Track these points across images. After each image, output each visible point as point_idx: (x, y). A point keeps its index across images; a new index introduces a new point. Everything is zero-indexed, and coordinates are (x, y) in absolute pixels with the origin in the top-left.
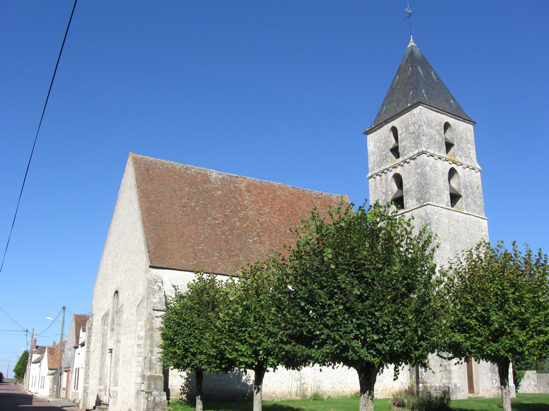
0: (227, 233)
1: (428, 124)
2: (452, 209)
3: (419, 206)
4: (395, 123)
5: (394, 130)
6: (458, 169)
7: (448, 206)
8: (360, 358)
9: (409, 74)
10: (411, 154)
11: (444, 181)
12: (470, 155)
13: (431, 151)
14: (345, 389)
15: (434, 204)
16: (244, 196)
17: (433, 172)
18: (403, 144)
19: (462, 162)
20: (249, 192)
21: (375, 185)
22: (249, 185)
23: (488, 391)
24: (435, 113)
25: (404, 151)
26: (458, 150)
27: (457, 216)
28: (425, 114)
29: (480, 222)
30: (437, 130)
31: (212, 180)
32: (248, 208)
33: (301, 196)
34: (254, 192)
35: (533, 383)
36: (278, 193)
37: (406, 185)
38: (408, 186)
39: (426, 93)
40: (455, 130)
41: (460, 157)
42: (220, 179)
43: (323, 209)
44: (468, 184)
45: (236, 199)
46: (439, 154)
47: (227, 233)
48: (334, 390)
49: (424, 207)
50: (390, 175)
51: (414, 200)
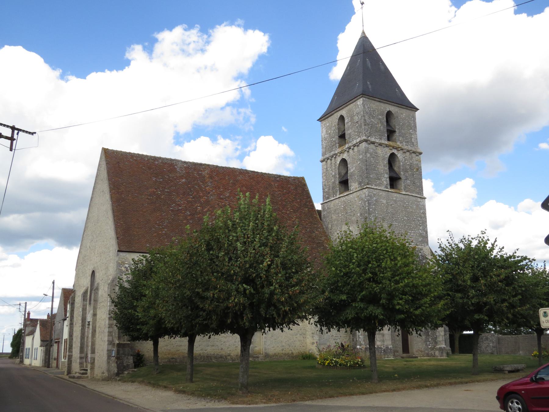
0: (189, 218)
1: (370, 114)
2: (393, 190)
3: (360, 188)
4: (343, 112)
5: (342, 118)
6: (399, 155)
7: (387, 188)
8: (321, 326)
9: (358, 64)
10: (355, 142)
11: (384, 166)
12: (411, 140)
13: (373, 139)
14: (294, 351)
15: (372, 187)
16: (206, 183)
17: (373, 158)
18: (349, 132)
19: (403, 147)
20: (212, 179)
21: (326, 168)
22: (212, 172)
23: (421, 351)
24: (378, 103)
25: (349, 138)
26: (400, 136)
27: (395, 197)
28: (367, 105)
29: (418, 202)
30: (379, 119)
31: (178, 169)
32: (209, 193)
33: (260, 179)
34: (217, 178)
35: (491, 345)
36: (239, 178)
37: (352, 169)
38: (352, 170)
39: (371, 84)
40: (397, 117)
41: (401, 143)
42: (185, 168)
43: (280, 191)
44: (408, 167)
45: (199, 186)
46: (380, 142)
47: (189, 218)
48: (284, 352)
49: (364, 190)
50: (339, 159)
51: (357, 184)
